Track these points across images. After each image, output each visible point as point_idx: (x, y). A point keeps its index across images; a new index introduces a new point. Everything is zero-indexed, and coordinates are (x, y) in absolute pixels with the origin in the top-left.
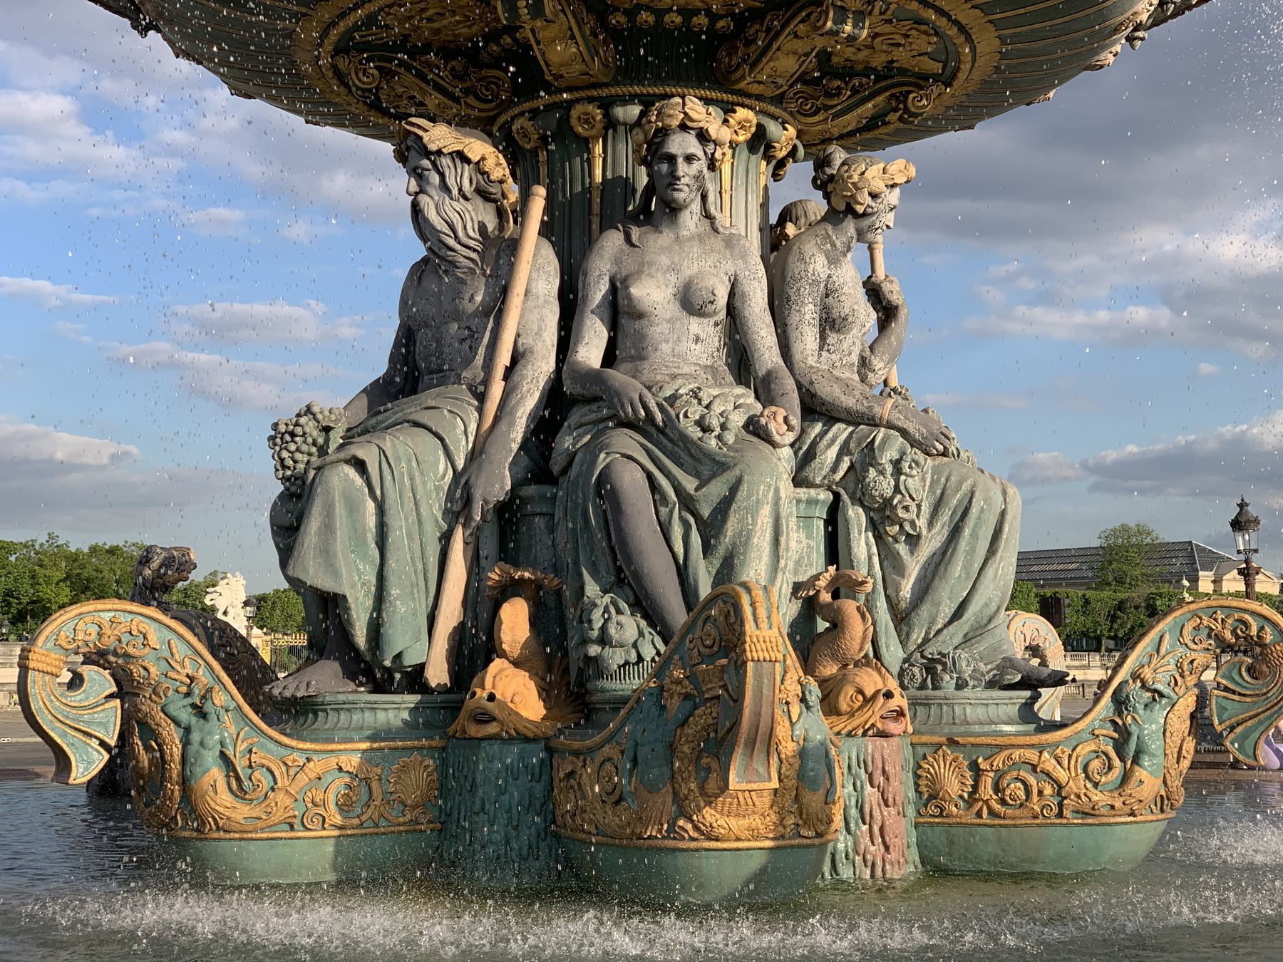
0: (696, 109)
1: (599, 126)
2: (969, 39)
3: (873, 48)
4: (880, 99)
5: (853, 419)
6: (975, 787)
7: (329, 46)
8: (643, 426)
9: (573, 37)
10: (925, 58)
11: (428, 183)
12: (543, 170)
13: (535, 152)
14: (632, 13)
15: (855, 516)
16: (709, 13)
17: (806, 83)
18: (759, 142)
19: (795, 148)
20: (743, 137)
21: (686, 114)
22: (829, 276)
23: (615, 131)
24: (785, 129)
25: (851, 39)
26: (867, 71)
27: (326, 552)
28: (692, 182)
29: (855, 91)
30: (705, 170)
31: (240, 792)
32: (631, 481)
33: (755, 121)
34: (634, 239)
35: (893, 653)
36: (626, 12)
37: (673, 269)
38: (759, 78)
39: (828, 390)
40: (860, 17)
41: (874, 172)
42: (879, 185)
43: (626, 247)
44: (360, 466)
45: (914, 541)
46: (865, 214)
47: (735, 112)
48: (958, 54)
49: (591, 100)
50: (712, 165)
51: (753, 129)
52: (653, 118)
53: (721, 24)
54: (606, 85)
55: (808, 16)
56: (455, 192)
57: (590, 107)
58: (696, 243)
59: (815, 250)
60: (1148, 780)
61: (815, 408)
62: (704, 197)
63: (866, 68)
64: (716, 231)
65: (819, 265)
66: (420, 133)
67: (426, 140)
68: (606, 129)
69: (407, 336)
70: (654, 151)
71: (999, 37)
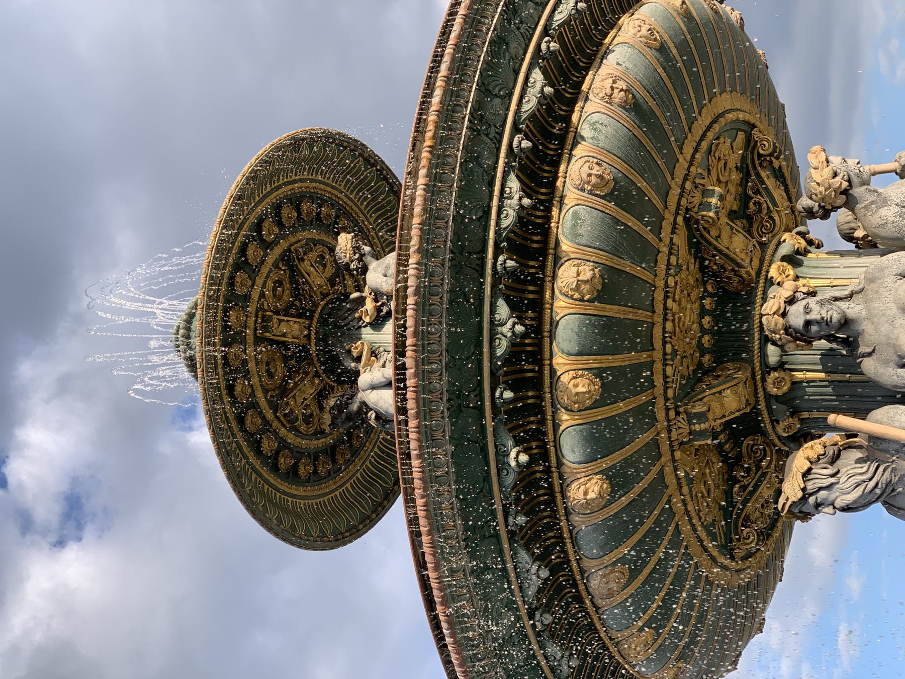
0: (771, 306)
1: (782, 374)
2: (721, 115)
3: (727, 182)
4: (763, 174)
7: (726, 561)
9: (720, 393)
10: (734, 144)
11: (826, 499)
12: (815, 414)
13: (802, 421)
16: (703, 298)
17: (751, 226)
18: (794, 259)
19: (798, 233)
20: (791, 272)
21: (774, 314)
22: (897, 205)
23: (786, 363)
24: (784, 241)
25: (722, 198)
26: (744, 183)
28: (825, 309)
29: (758, 192)
30: (816, 299)
33: (779, 263)
34: (869, 350)
36: (702, 356)
37: (892, 322)
38: (748, 261)
40: (706, 193)
41: (817, 176)
42: (827, 172)
43: (874, 356)
46: (849, 181)
47: (772, 278)
48: (732, 121)
49: (764, 380)
50: (813, 294)
51: (785, 264)
52: (778, 336)
53: (710, 288)
54: (753, 369)
55: (705, 228)
56: (832, 480)
58: (872, 305)
59: (876, 216)
62: (836, 299)
63: (740, 185)
64: (862, 290)
65: (889, 213)
66: (789, 503)
67: (795, 500)
68: (785, 370)
70: (803, 336)
71: (721, 94)
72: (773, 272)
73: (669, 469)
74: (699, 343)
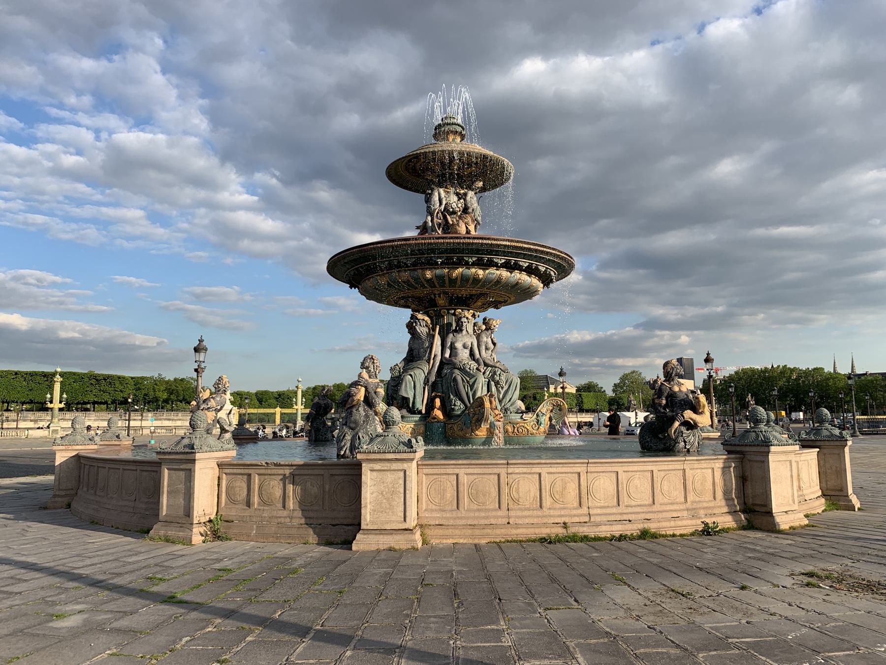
5: (492, 366)
8: (460, 369)
15: (493, 383)
27: (406, 390)
32: (459, 378)
35: (499, 408)
39: (487, 361)
44: (411, 375)
45: (502, 388)
60: (542, 428)
61: (486, 365)
65: (485, 339)
69: (411, 351)
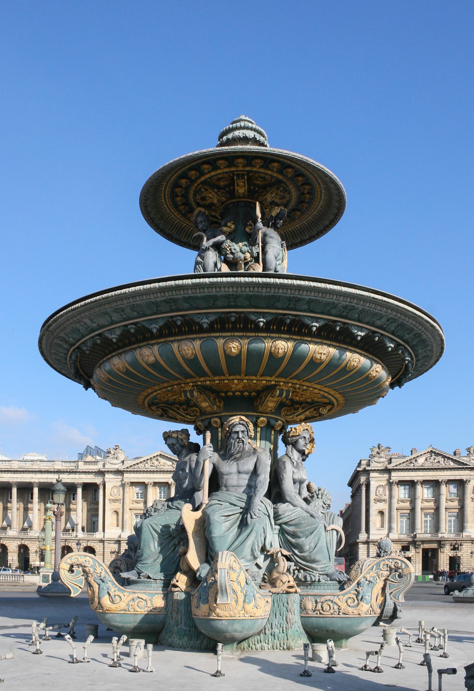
1: (219, 424)
6: (316, 607)
14: (226, 393)
16: (247, 391)
26: (307, 403)
31: (113, 602)
49: (216, 417)
57: (216, 419)
72: (262, 419)
73: (170, 384)
74: (229, 391)
